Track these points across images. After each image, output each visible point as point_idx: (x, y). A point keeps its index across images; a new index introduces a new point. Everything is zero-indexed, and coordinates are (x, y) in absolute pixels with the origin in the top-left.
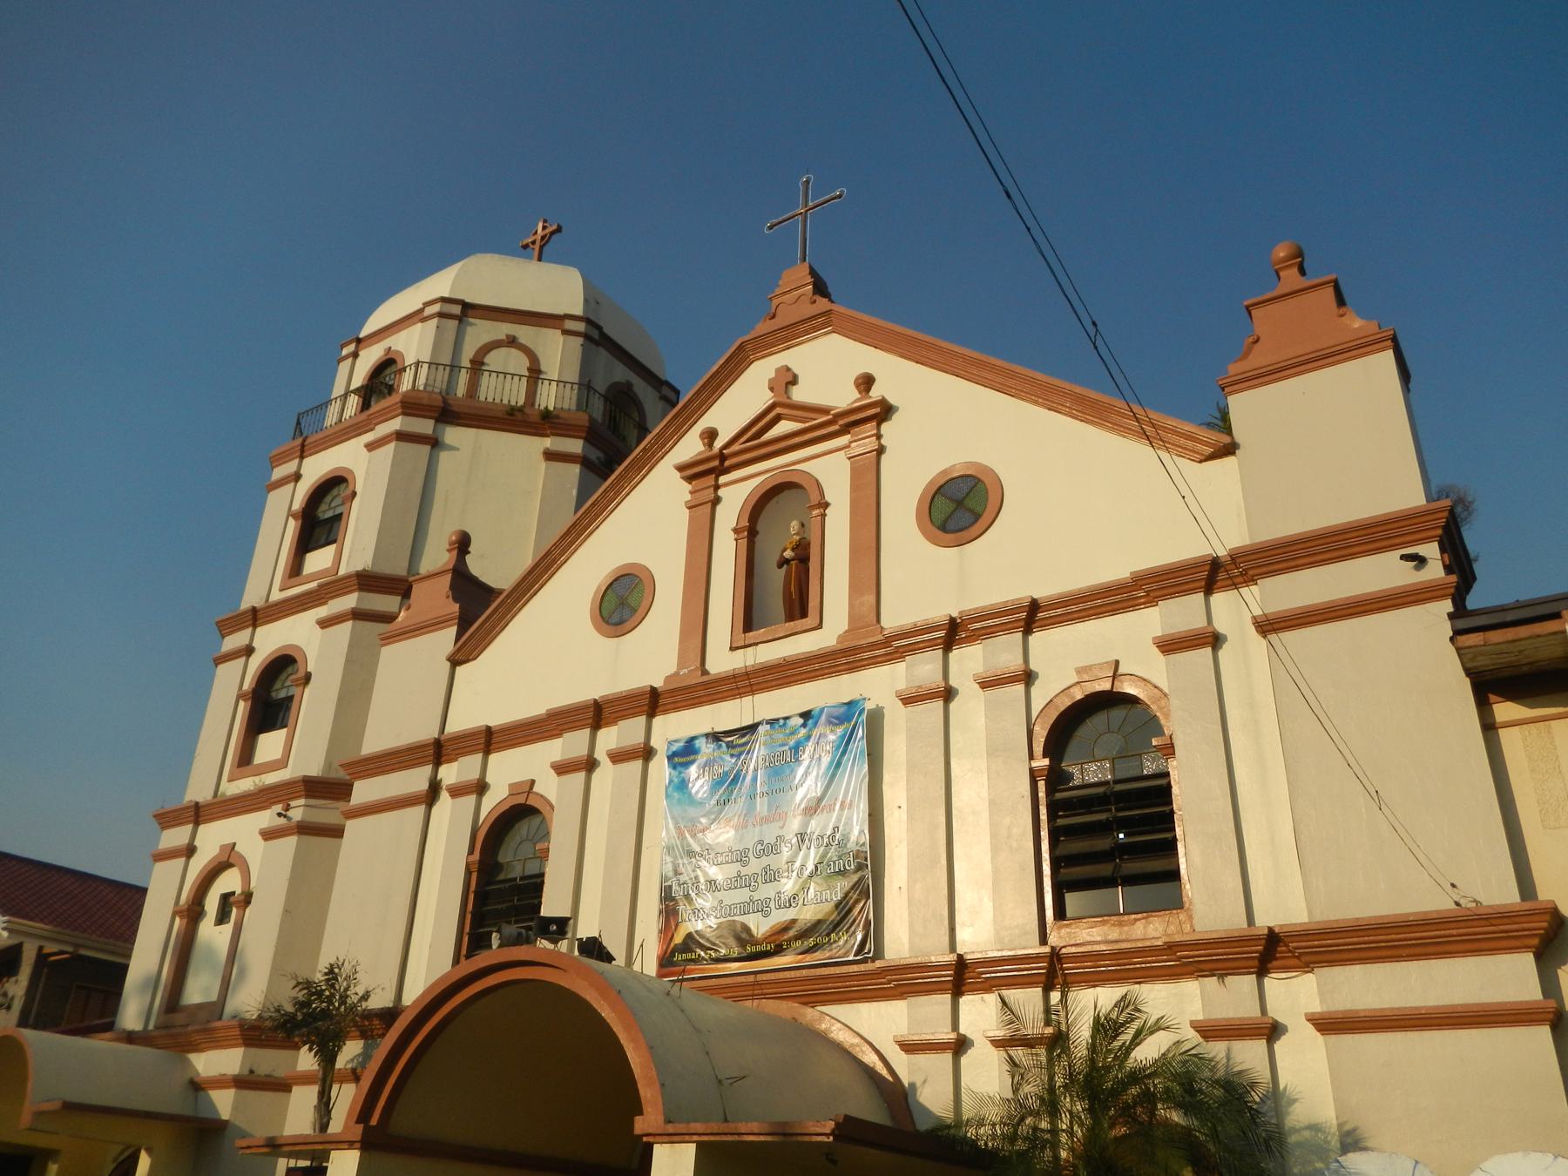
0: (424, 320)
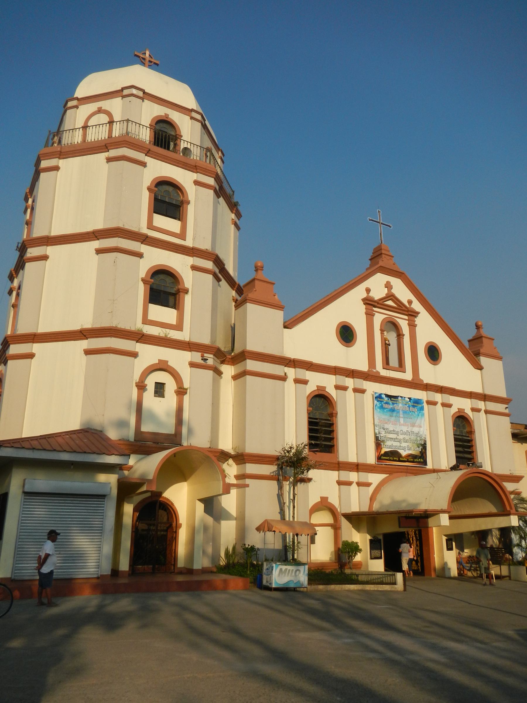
0: (192, 118)
